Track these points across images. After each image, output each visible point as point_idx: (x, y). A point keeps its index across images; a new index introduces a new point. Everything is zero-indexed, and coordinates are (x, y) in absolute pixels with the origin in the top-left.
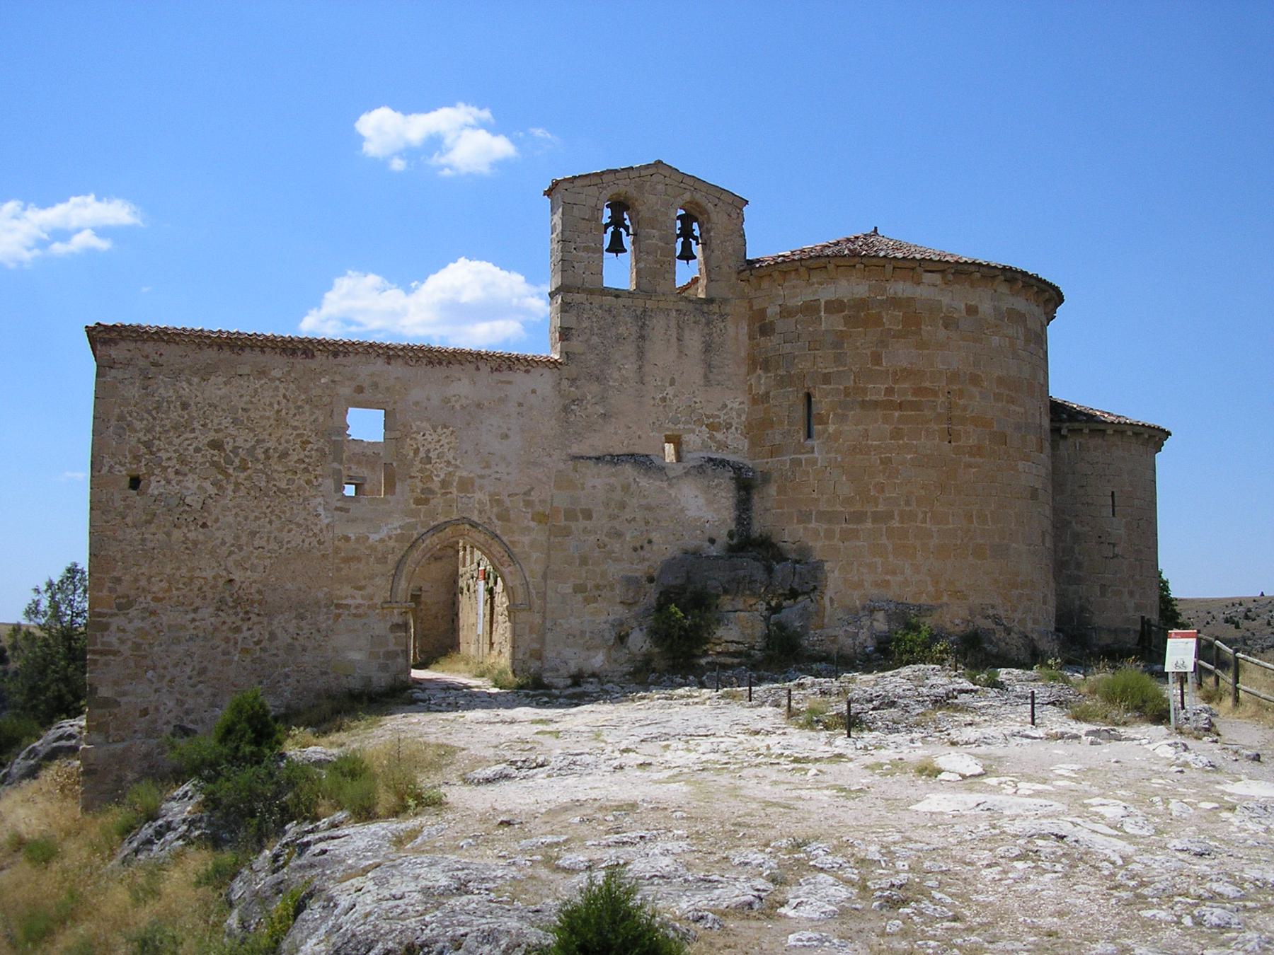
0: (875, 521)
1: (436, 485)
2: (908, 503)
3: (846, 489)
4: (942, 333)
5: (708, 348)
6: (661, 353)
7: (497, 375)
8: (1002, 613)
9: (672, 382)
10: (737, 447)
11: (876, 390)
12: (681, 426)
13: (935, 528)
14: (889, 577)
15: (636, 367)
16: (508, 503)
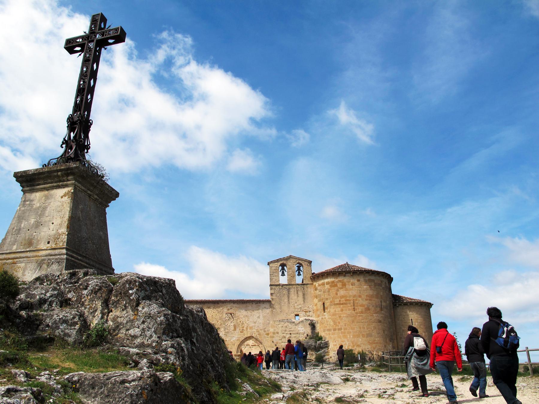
1: (245, 329)
3: (332, 323)
4: (351, 286)
5: (304, 295)
6: (293, 296)
11: (337, 301)
16: (260, 331)
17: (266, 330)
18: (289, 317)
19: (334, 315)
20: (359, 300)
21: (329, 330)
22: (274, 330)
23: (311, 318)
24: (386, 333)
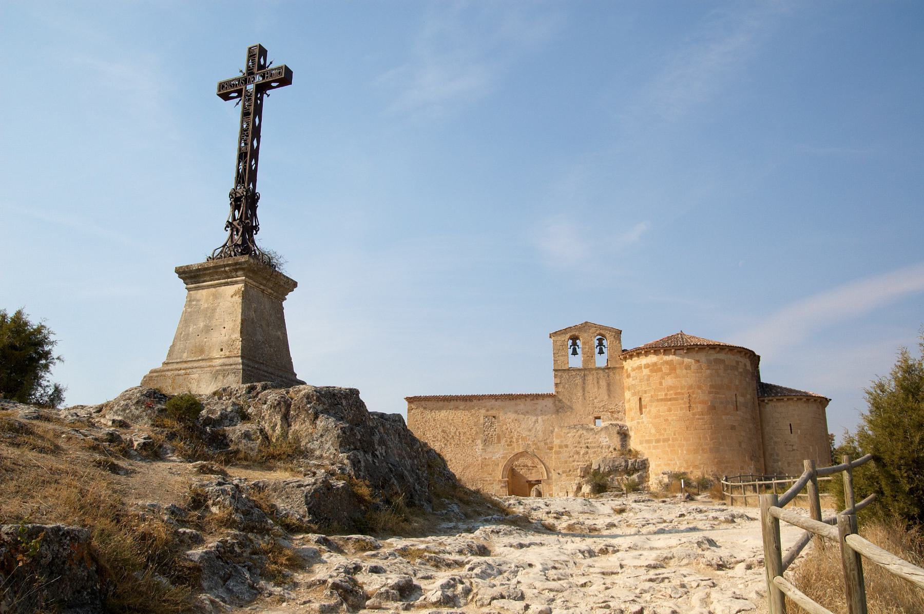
3: (653, 431)
4: (685, 371)
5: (609, 385)
11: (661, 395)
17: (548, 441)
18: (584, 421)
21: (648, 442)
22: (562, 441)
23: (620, 423)
24: (744, 446)
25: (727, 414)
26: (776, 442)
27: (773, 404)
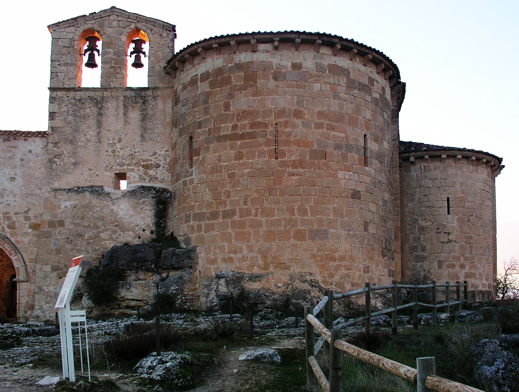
0: (224, 217)
2: (245, 203)
3: (208, 197)
4: (272, 83)
5: (144, 118)
7: (7, 143)
8: (319, 278)
9: (120, 141)
10: (162, 179)
11: (226, 128)
12: (125, 167)
13: (264, 219)
14: (232, 255)
15: (96, 133)
16: (14, 218)
19: (215, 170)
20: (295, 126)
21: (199, 217)
23: (158, 185)
25: (347, 169)
26: (422, 229)
27: (423, 164)
